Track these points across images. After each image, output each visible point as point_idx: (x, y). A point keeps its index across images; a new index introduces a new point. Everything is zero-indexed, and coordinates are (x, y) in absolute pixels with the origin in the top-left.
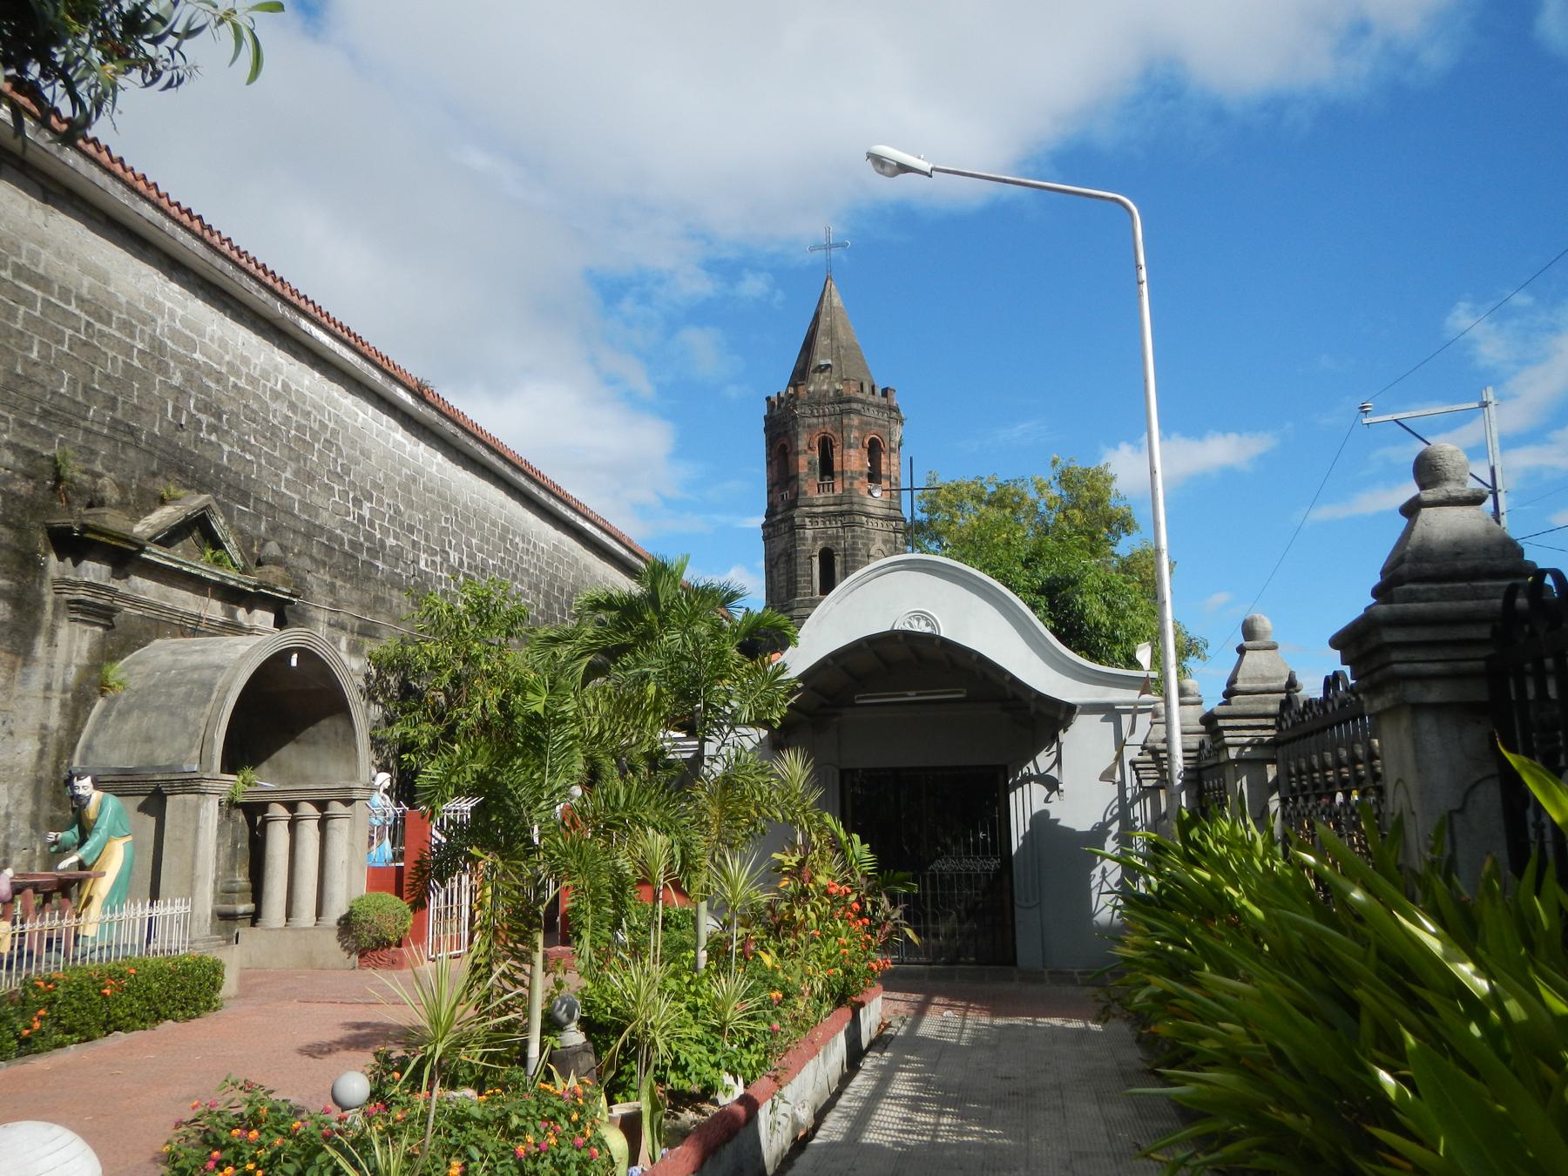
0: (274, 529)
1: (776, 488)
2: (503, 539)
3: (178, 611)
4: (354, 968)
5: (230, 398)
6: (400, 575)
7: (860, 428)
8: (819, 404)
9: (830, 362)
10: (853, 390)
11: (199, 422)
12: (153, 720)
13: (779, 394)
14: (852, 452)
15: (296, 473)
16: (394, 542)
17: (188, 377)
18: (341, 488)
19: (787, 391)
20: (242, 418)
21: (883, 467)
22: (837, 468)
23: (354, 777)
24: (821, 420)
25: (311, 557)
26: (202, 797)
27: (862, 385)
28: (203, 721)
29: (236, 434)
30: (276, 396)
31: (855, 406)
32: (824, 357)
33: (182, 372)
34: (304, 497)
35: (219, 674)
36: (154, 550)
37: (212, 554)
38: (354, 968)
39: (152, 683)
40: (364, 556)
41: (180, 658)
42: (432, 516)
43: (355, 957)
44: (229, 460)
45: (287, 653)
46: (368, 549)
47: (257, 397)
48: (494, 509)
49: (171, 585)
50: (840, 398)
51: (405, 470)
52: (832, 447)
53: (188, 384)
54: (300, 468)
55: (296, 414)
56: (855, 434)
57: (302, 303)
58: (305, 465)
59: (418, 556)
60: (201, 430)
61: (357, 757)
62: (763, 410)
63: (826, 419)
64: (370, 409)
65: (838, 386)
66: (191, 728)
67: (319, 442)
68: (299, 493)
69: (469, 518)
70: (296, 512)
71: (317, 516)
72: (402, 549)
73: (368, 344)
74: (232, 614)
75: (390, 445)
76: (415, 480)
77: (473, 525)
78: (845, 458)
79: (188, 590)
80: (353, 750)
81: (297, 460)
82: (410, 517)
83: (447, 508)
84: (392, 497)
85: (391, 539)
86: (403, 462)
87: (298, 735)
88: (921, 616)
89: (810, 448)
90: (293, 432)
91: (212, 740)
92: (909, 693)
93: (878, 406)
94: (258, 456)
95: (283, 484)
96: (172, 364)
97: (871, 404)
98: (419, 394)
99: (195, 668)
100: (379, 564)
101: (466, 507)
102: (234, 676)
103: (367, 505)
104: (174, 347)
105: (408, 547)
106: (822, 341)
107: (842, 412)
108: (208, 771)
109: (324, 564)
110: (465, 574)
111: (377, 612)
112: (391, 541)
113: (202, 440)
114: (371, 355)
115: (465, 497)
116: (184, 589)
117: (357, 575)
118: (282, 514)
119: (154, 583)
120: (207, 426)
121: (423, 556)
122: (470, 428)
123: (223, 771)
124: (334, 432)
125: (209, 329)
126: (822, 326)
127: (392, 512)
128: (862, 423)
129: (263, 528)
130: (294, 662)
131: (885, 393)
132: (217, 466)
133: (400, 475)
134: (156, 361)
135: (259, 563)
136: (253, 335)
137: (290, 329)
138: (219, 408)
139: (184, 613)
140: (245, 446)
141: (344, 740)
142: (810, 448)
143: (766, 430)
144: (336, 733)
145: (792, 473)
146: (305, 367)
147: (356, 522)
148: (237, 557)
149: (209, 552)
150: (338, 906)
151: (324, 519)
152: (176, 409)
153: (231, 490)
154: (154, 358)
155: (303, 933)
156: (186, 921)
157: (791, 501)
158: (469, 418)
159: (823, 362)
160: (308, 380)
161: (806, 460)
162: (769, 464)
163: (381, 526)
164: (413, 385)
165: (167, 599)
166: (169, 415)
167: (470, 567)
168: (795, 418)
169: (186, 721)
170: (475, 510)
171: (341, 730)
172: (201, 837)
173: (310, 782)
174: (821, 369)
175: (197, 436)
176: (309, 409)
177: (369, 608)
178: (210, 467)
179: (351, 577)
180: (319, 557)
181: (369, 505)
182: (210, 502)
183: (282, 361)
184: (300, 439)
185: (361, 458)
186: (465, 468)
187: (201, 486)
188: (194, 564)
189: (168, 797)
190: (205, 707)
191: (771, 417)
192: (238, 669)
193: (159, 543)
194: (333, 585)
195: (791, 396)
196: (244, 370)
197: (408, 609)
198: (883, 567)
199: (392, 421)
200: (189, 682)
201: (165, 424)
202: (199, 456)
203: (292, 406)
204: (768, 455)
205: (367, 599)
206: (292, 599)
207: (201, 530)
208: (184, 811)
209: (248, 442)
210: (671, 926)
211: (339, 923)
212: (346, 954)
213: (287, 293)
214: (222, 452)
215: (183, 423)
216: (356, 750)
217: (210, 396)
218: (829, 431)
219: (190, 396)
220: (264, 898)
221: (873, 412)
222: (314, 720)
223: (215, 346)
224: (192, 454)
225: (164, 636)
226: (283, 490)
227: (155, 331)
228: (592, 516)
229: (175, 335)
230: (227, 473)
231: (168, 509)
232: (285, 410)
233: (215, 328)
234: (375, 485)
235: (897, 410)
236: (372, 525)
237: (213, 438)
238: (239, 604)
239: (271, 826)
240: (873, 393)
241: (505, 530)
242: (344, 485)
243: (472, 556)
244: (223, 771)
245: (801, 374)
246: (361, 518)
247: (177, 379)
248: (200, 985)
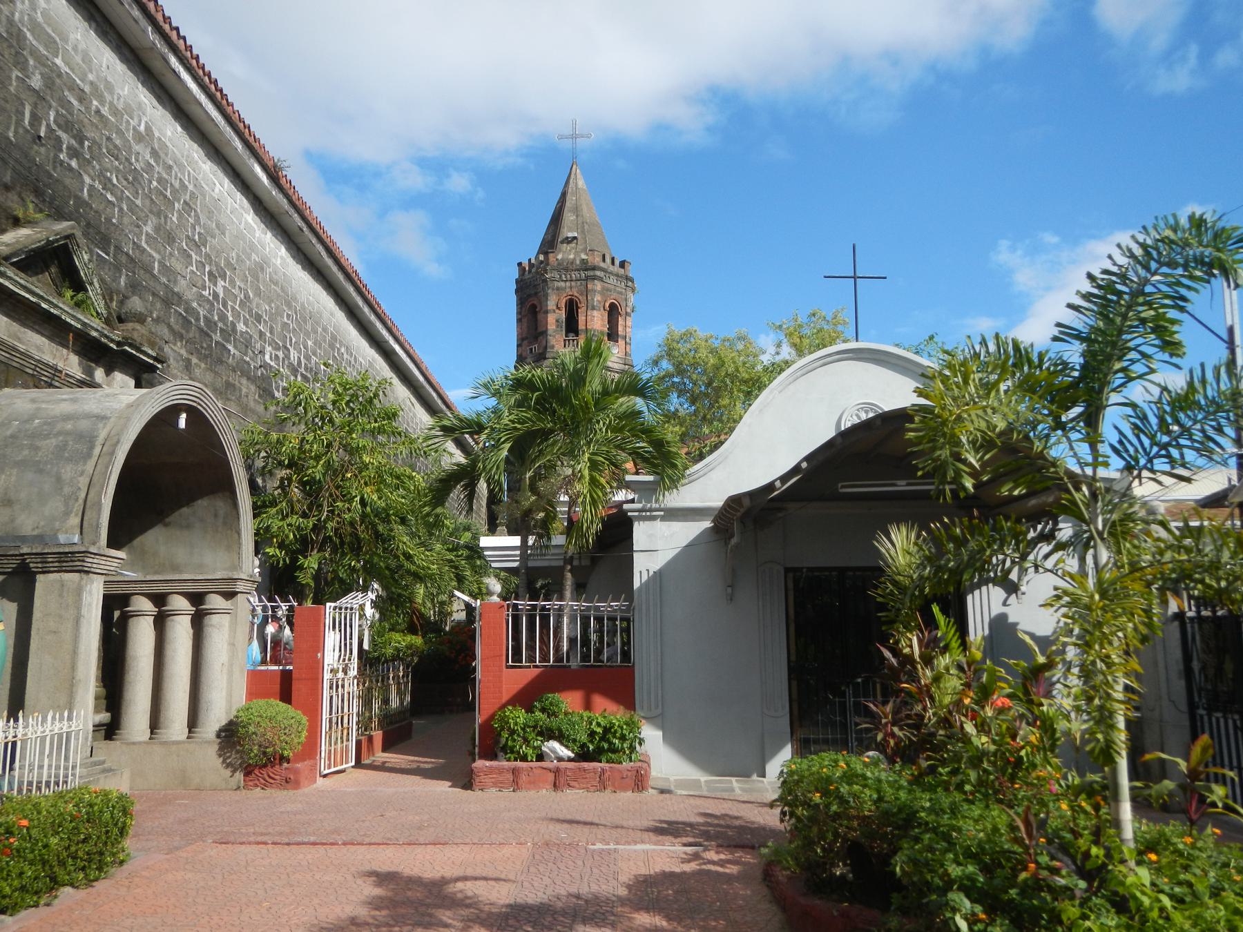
0: (134, 287)
1: (526, 342)
2: (332, 346)
3: (32, 358)
4: (238, 788)
5: (92, 124)
6: (248, 363)
7: (601, 293)
8: (566, 269)
9: (576, 234)
10: (597, 260)
11: (59, 140)
12: (13, 478)
13: (530, 260)
14: (595, 313)
15: (157, 229)
16: (244, 329)
17: (49, 83)
18: (198, 259)
19: (537, 258)
20: (105, 151)
21: (620, 328)
22: (581, 326)
23: (237, 567)
24: (568, 284)
25: (169, 326)
26: (83, 575)
27: (604, 256)
28: (83, 482)
29: (97, 167)
30: (139, 138)
31: (598, 273)
32: (570, 231)
33: (41, 74)
34: (163, 258)
35: (101, 425)
36: (10, 273)
37: (72, 297)
38: (238, 788)
39: (9, 433)
40: (217, 337)
41: (44, 406)
42: (277, 308)
43: (239, 776)
44: (90, 195)
45: (173, 411)
46: (222, 330)
47: (120, 133)
48: (326, 315)
49: (24, 325)
50: (586, 266)
51: (254, 256)
52: (578, 308)
53: (49, 92)
54: (160, 224)
55: (158, 165)
56: (598, 298)
57: (174, 35)
58: (166, 223)
59: (264, 348)
60: (61, 150)
61: (240, 544)
62: (515, 274)
63: (573, 283)
64: (226, 182)
65: (584, 256)
66: (67, 490)
67: (179, 203)
68: (159, 253)
69: (306, 318)
70: (156, 272)
71: (175, 282)
72: (251, 336)
73: (232, 105)
74: (90, 372)
75: (242, 227)
76: (262, 269)
77: (309, 327)
78: (589, 318)
79: (43, 335)
80: (236, 535)
81: (158, 214)
82: (258, 306)
83: (289, 305)
84: (243, 281)
85: (242, 325)
86: (252, 247)
87: (168, 516)
88: (868, 406)
89: (558, 308)
90: (155, 183)
91: (99, 505)
92: (899, 482)
93: (617, 275)
94: (120, 199)
95: (143, 238)
96: (31, 62)
97: (611, 273)
98: (274, 175)
99: (67, 418)
100: (231, 347)
101: (303, 304)
102: (125, 427)
103: (221, 283)
104: (34, 42)
105: (256, 336)
106: (569, 217)
107: (587, 278)
108: (94, 544)
109: (181, 337)
110: (302, 375)
111: (228, 399)
112: (241, 327)
113: (62, 162)
114: (235, 117)
115: (303, 297)
116: (39, 332)
117: (211, 355)
118: (142, 272)
119: (5, 319)
120: (69, 148)
121: (268, 349)
122: (314, 225)
123: (108, 546)
124: (192, 194)
125: (72, 36)
126: (568, 204)
127: (242, 296)
128: (603, 288)
129: (122, 283)
130: (182, 423)
131: (622, 264)
132: (78, 199)
133: (250, 260)
134: (13, 51)
135: (121, 320)
136: (118, 62)
137: (157, 65)
138: (81, 131)
139: (39, 361)
140: (107, 184)
141: (225, 523)
142: (558, 308)
143: (517, 291)
144: (216, 516)
145: (540, 329)
146: (168, 116)
147: (211, 298)
148: (100, 306)
149: (69, 293)
150: (217, 714)
151: (181, 286)
152: (35, 119)
153: (91, 230)
154: (11, 46)
155: (174, 748)
156: (63, 741)
157: (540, 354)
158: (315, 215)
159: (570, 235)
160: (170, 131)
161: (554, 319)
162: (519, 321)
163: (233, 308)
164: (270, 164)
165: (19, 340)
166: (27, 122)
167: (306, 369)
168: (545, 281)
169: (59, 479)
170: (310, 312)
171: (221, 512)
172: (83, 630)
173: (181, 572)
174: (568, 241)
175: (56, 156)
176: (171, 163)
177: (221, 393)
178: (69, 197)
179: (206, 357)
180: (177, 327)
181: (223, 283)
182: (74, 231)
183: (146, 101)
184: (161, 193)
185: (217, 232)
186: (304, 268)
187: (59, 215)
188: (55, 301)
189: (40, 578)
190: (85, 464)
191: (522, 280)
192: (128, 419)
193: (13, 264)
194: (188, 361)
195: (542, 262)
196: (108, 97)
197: (255, 400)
198: (830, 355)
199: (245, 201)
200: (59, 433)
201: (21, 131)
202: (57, 181)
203: (154, 153)
204: (519, 313)
205: (219, 383)
206: (156, 364)
207: (60, 266)
208: (61, 596)
209: (110, 180)
210: (615, 737)
211: (218, 736)
212: (228, 772)
213: (160, 18)
214: (83, 182)
215: (42, 134)
216: (239, 534)
217: (72, 115)
218: (576, 294)
219: (50, 107)
220: (124, 708)
221: (612, 280)
222: (190, 500)
223: (78, 59)
224: (51, 176)
225: (15, 386)
226: (145, 246)
227: (13, 14)
228: (401, 339)
229: (35, 27)
230: (87, 209)
231: (23, 232)
232: (148, 157)
233: (79, 37)
234: (229, 264)
235: (632, 280)
236: (225, 305)
237: (74, 163)
238: (98, 362)
239: (133, 622)
240: (613, 263)
241: (334, 338)
242: (201, 256)
243: (308, 358)
244: (108, 546)
245: (550, 243)
246: (216, 295)
247: (36, 82)
248: (107, 832)
